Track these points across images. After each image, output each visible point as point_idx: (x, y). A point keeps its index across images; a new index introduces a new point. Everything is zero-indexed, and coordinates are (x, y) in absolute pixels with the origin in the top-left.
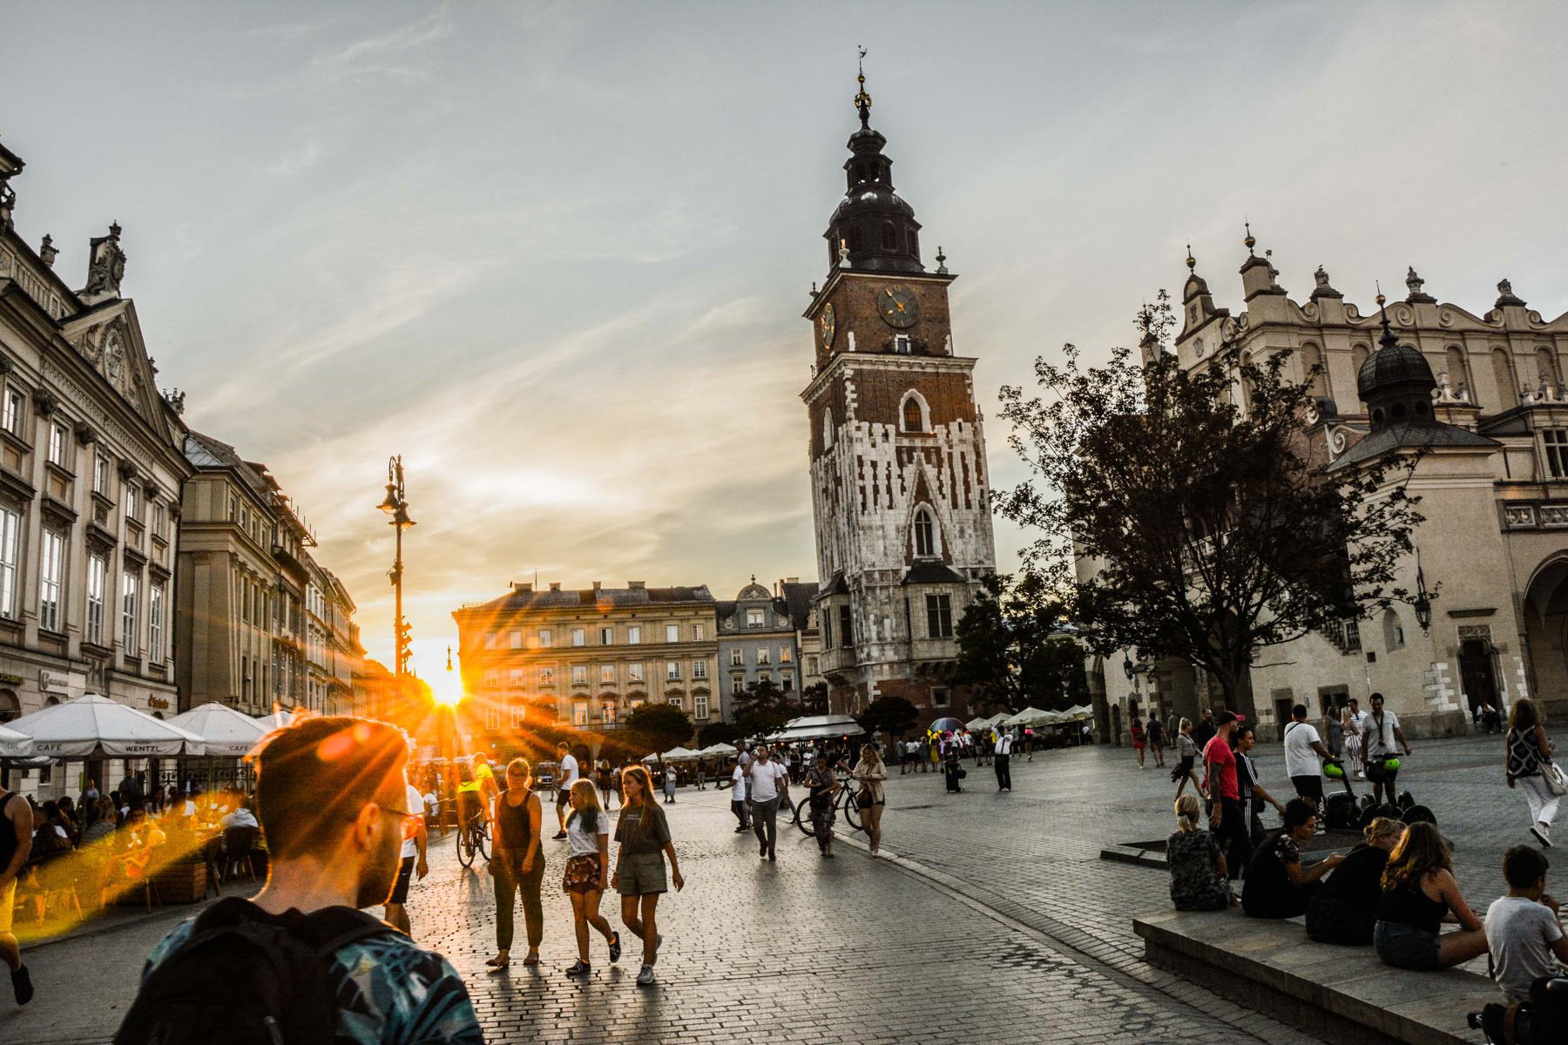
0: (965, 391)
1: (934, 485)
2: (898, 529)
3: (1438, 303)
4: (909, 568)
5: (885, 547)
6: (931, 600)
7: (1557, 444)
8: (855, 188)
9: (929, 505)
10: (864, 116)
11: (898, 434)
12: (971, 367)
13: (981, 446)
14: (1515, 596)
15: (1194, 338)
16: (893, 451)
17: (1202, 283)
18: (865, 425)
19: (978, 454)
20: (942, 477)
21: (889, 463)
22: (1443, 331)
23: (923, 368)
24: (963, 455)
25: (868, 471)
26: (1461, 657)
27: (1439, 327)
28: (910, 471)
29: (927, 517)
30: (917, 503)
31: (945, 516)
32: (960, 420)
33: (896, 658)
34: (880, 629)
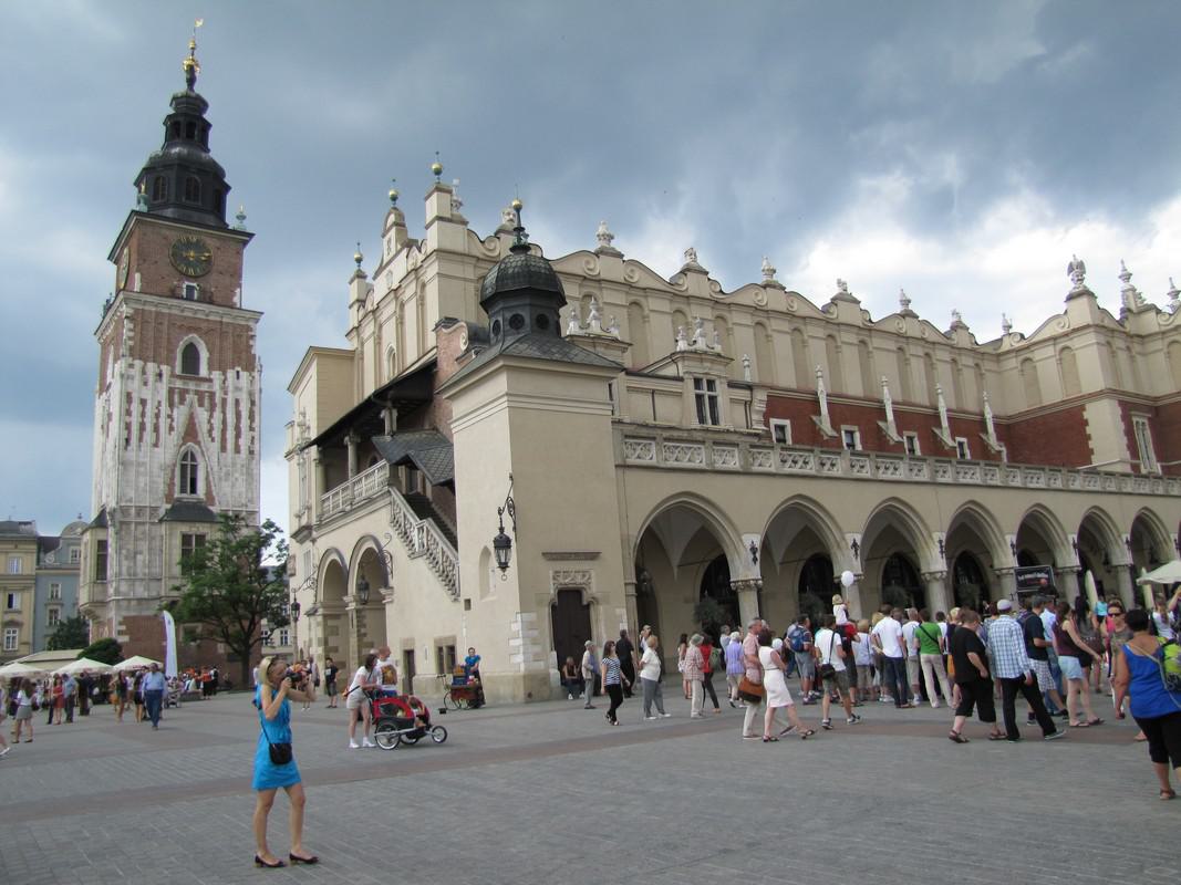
0: (248, 342)
1: (203, 427)
2: (161, 468)
3: (625, 259)
4: (169, 506)
5: (146, 485)
6: (186, 539)
7: (705, 391)
9: (197, 447)
11: (173, 375)
12: (257, 321)
13: (257, 396)
14: (624, 541)
15: (385, 272)
17: (400, 216)
18: (138, 363)
19: (253, 403)
20: (212, 421)
21: (159, 402)
22: (629, 286)
23: (207, 315)
24: (237, 402)
25: (135, 407)
26: (554, 608)
27: (623, 281)
28: (180, 414)
29: (193, 458)
31: (210, 459)
32: (239, 369)
33: (146, 595)
34: (132, 564)
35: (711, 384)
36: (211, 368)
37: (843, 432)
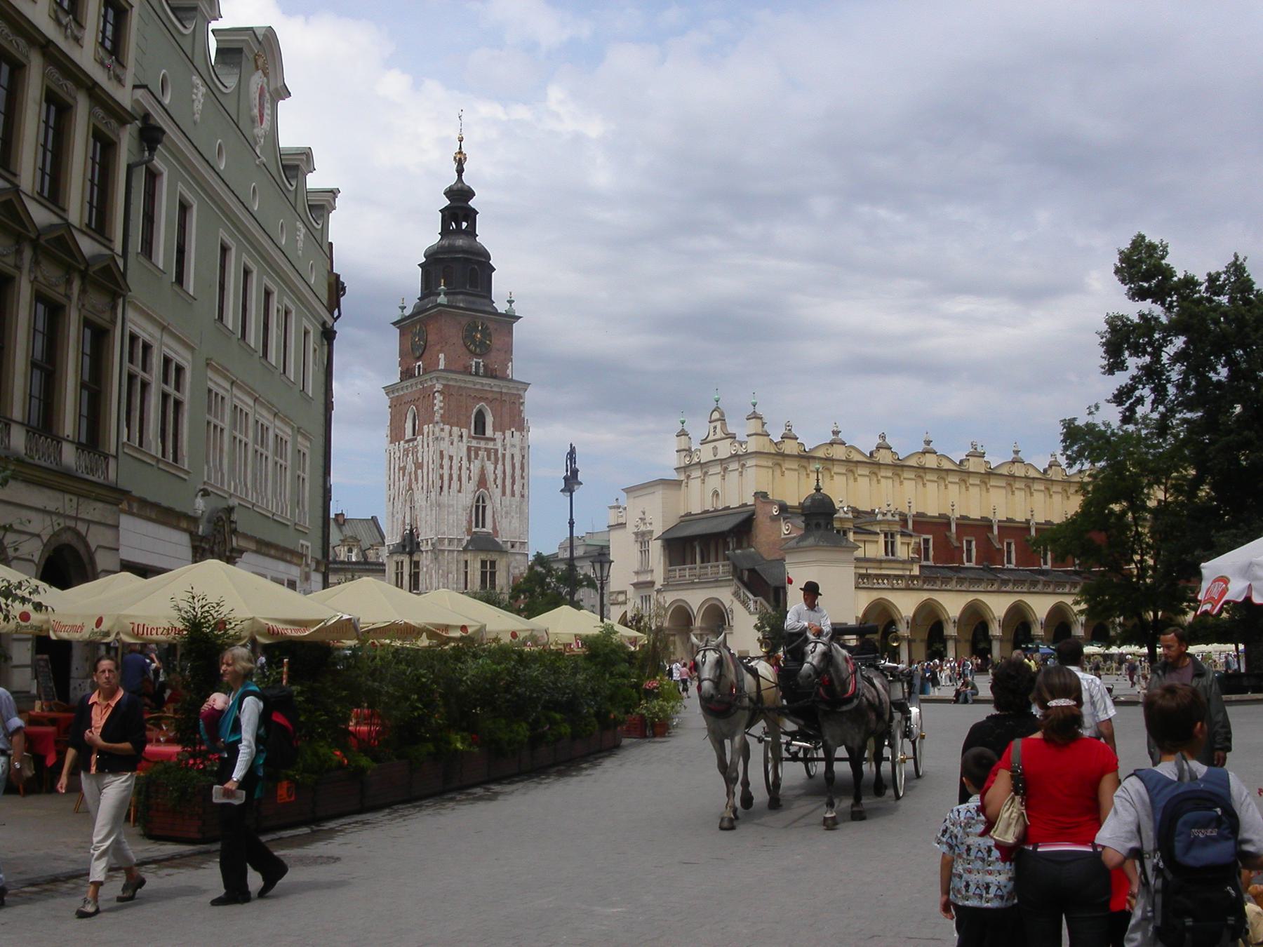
1: (491, 478)
4: (469, 538)
6: (484, 563)
7: (889, 539)
8: (445, 232)
10: (460, 171)
11: (469, 436)
14: (857, 617)
16: (465, 449)
17: (722, 414)
18: (447, 428)
20: (497, 472)
21: (461, 458)
25: (446, 462)
28: (475, 467)
30: (478, 490)
32: (513, 429)
35: (892, 535)
36: (494, 430)
37: (964, 542)
